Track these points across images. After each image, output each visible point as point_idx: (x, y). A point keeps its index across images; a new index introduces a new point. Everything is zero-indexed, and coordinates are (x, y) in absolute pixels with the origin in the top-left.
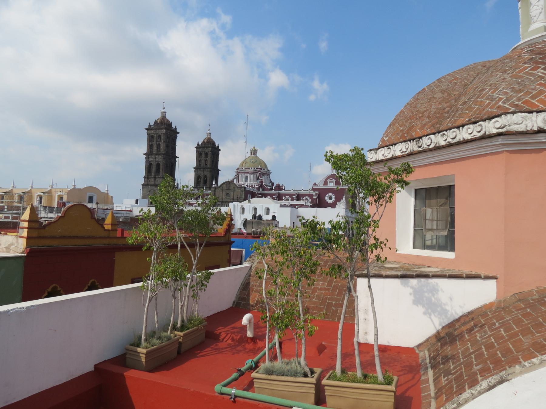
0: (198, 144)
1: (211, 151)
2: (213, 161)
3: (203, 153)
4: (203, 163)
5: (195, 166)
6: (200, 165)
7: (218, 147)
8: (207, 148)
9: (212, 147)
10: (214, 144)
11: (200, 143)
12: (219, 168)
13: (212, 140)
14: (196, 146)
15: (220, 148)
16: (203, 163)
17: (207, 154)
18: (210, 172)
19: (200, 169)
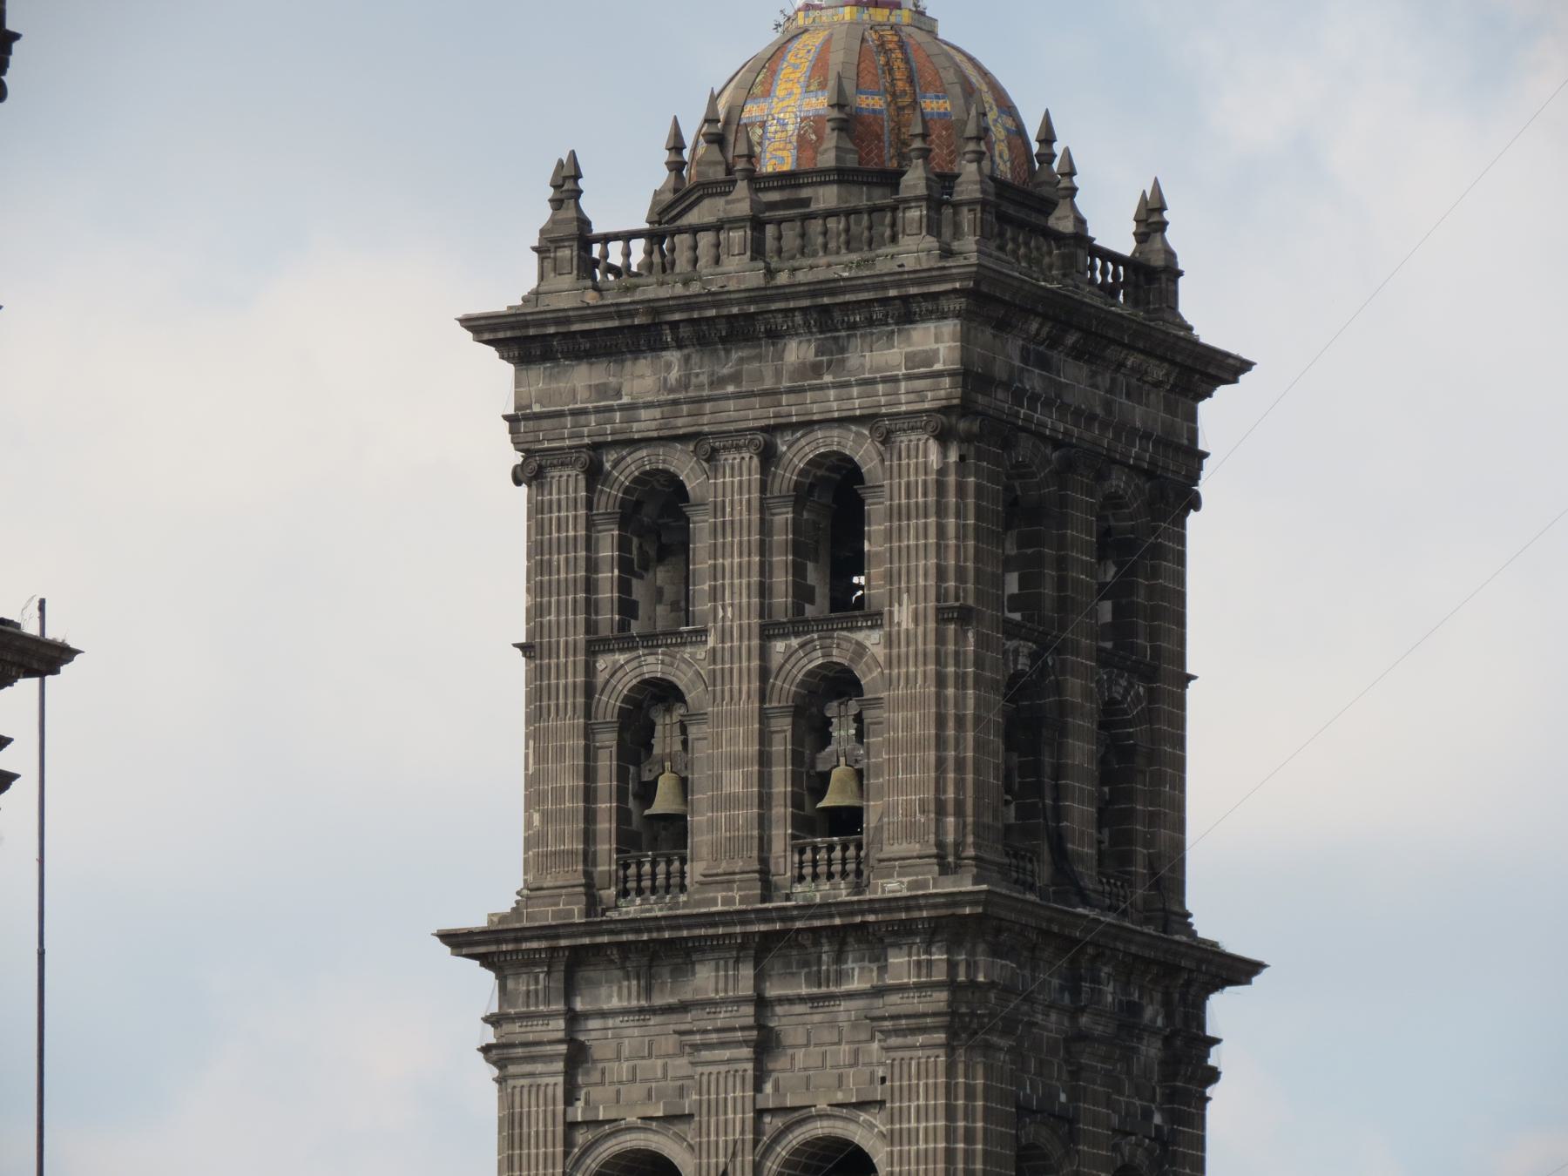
0: (570, 240)
1: (976, 418)
2: (1024, 724)
3: (726, 496)
4: (725, 778)
5: (493, 888)
6: (656, 837)
7: (1153, 274)
8: (836, 317)
9: (985, 305)
10: (1030, 195)
11: (620, 202)
12: (1214, 910)
13: (981, 92)
14: (511, 282)
15: (1206, 311)
16: (725, 778)
17: (832, 511)
18: (963, 1027)
19: (659, 954)
